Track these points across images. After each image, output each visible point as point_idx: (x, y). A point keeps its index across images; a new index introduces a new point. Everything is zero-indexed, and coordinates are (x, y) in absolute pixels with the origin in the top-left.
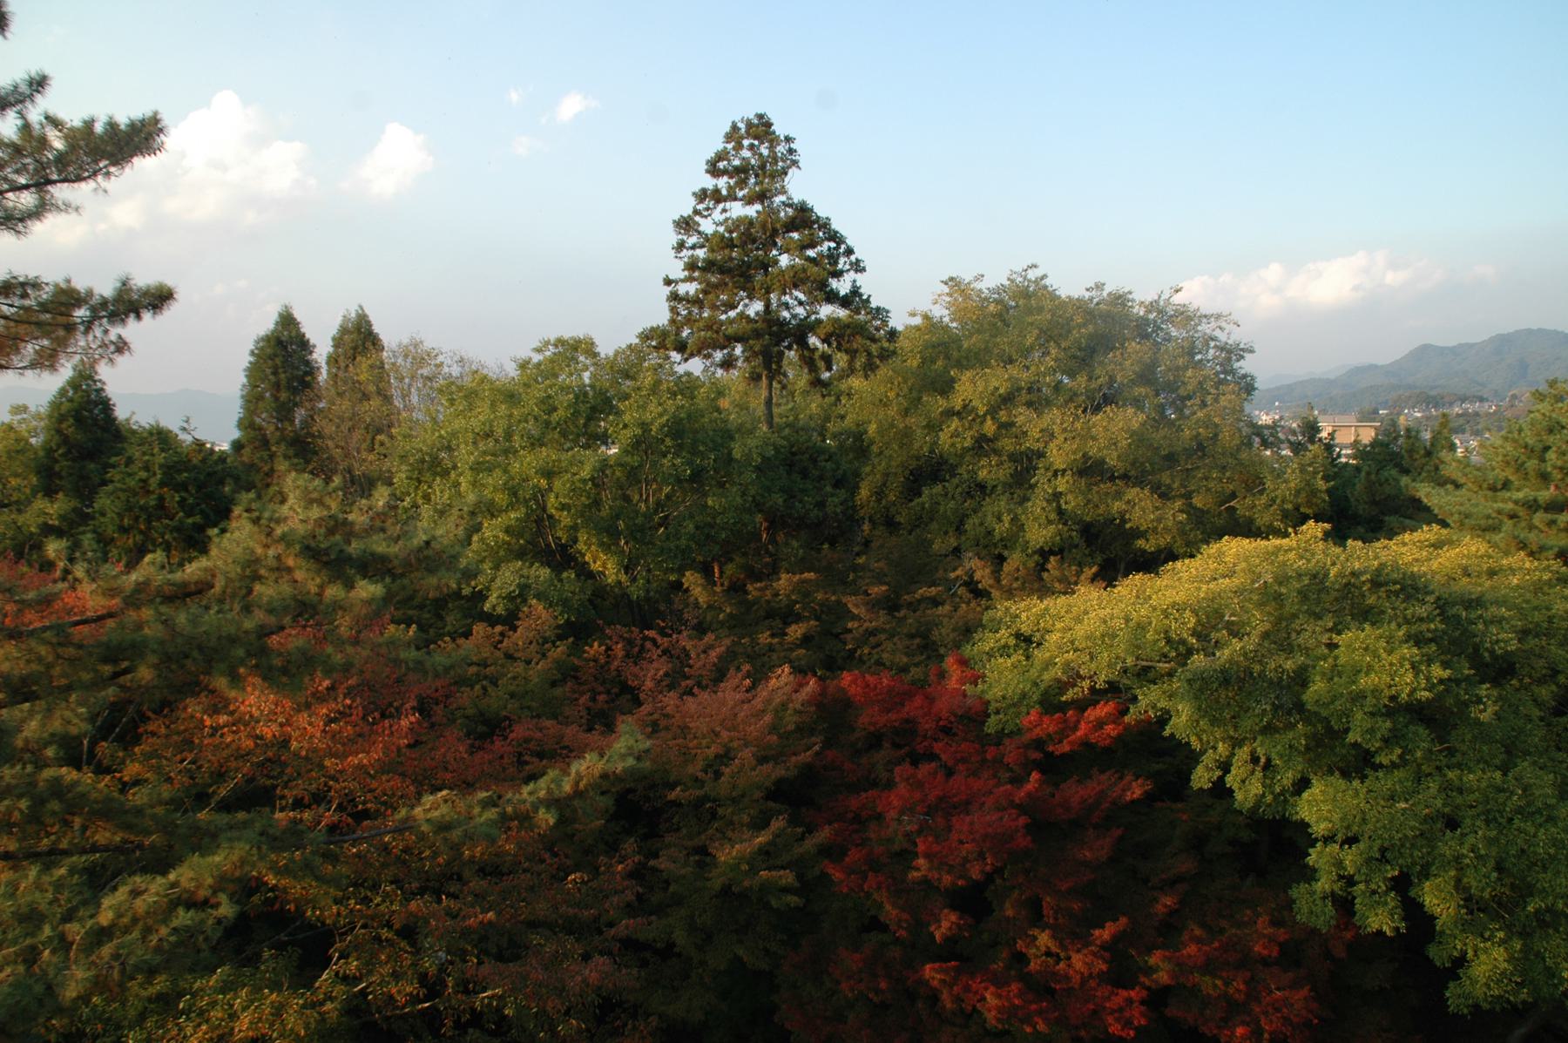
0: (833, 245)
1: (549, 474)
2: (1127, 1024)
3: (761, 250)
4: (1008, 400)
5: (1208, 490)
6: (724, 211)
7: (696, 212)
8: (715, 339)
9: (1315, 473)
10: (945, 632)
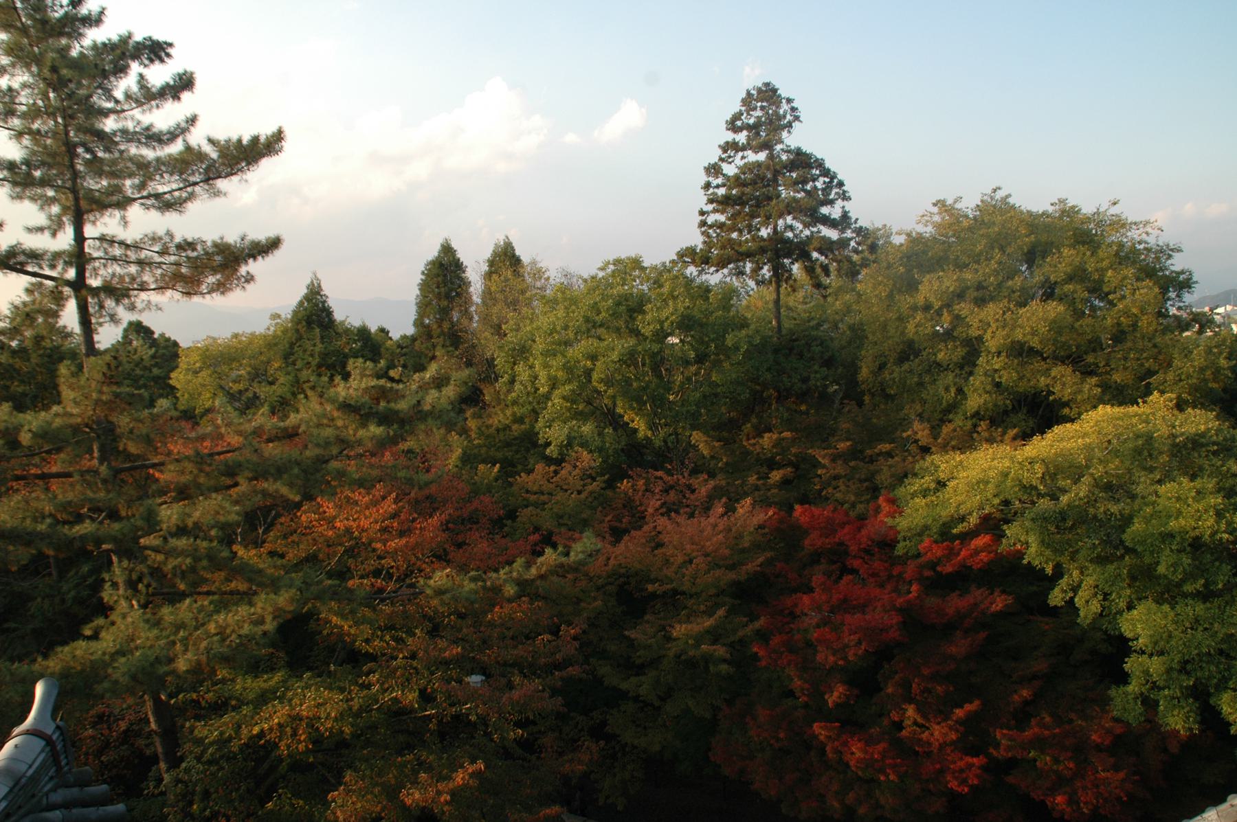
0: (827, 180)
2: (964, 782)
3: (769, 187)
4: (960, 295)
5: (1125, 369)
6: (743, 158)
7: (722, 160)
8: (730, 256)
9: (1220, 353)
10: (884, 477)
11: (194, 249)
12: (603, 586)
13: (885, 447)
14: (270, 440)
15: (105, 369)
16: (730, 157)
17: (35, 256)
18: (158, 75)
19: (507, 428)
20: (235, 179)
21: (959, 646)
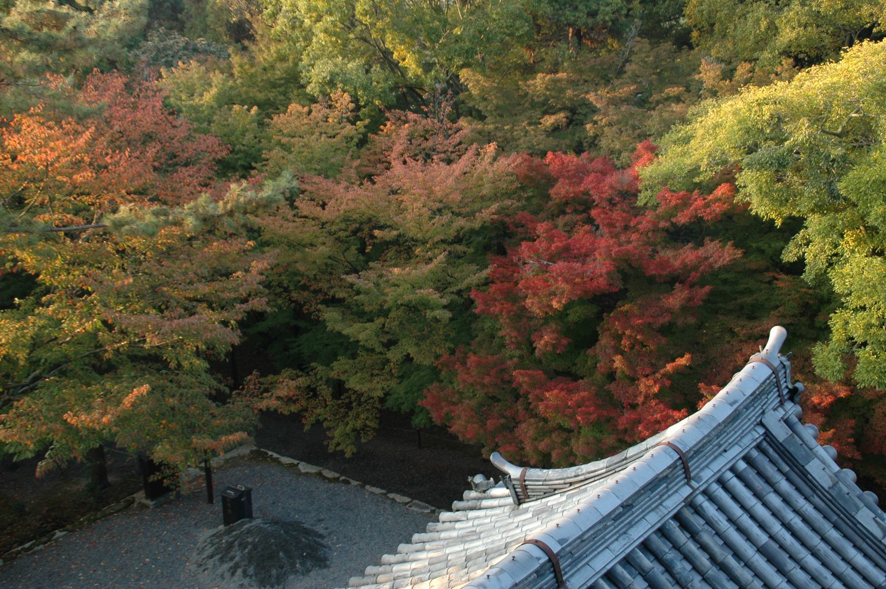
12: (335, 233)
13: (674, 91)
19: (272, 67)
21: (676, 299)
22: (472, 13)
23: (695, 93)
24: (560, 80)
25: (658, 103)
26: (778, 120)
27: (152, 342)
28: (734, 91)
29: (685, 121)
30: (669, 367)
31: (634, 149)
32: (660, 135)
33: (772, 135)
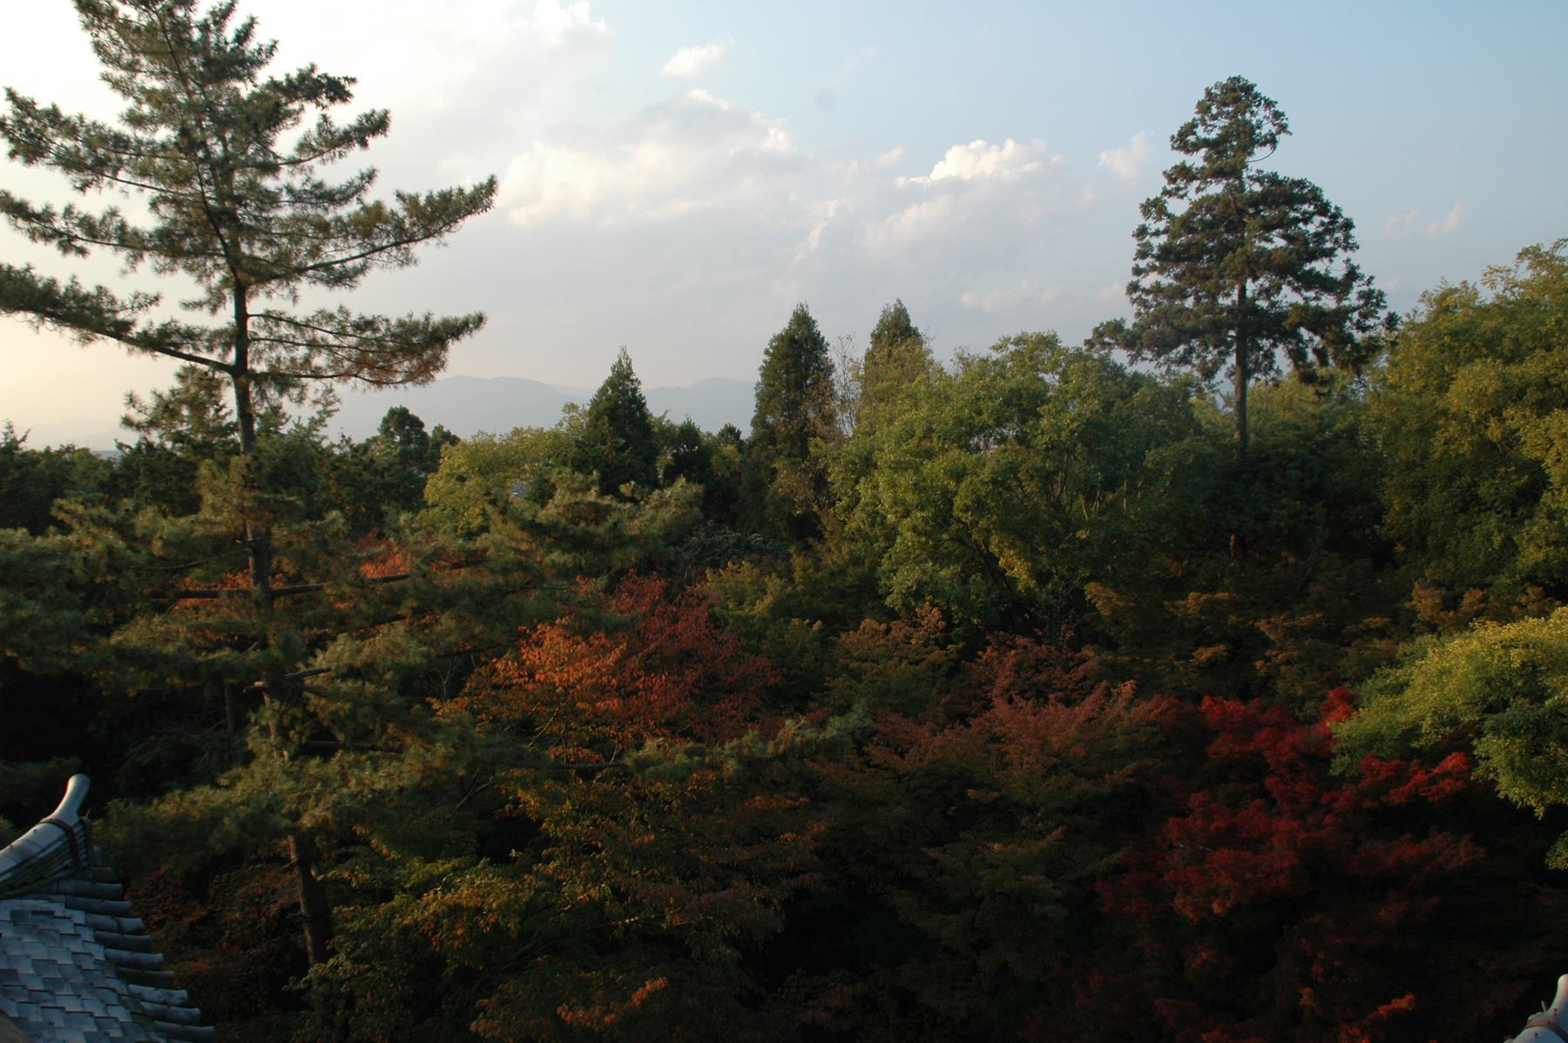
0: (1326, 220)
1: (958, 476)
3: (1239, 228)
7: (1166, 192)
11: (376, 330)
13: (1378, 621)
14: (457, 566)
15: (245, 472)
16: (1178, 189)
17: (190, 335)
18: (343, 116)
19: (843, 571)
20: (432, 241)
22: (1102, 512)
23: (1406, 626)
24: (1220, 602)
25: (1355, 636)
26: (1531, 670)
27: (672, 919)
28: (1463, 625)
29: (1394, 663)
30: (1382, 1010)
31: (1324, 697)
32: (1360, 680)
33: (1526, 690)
